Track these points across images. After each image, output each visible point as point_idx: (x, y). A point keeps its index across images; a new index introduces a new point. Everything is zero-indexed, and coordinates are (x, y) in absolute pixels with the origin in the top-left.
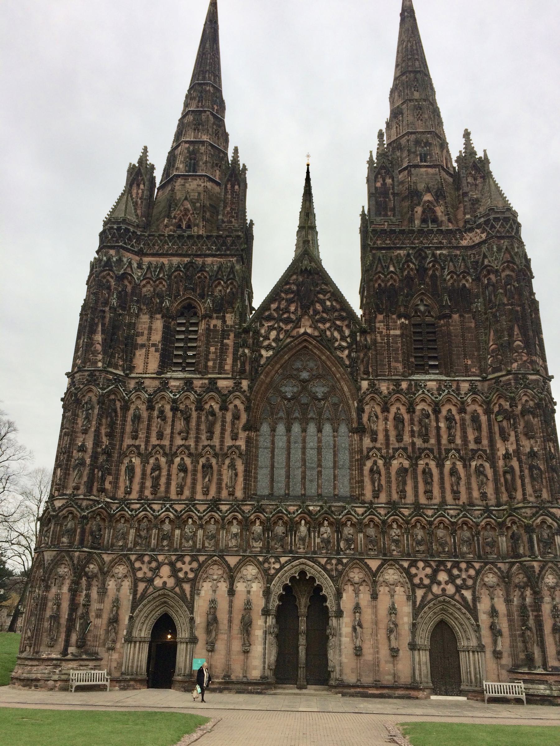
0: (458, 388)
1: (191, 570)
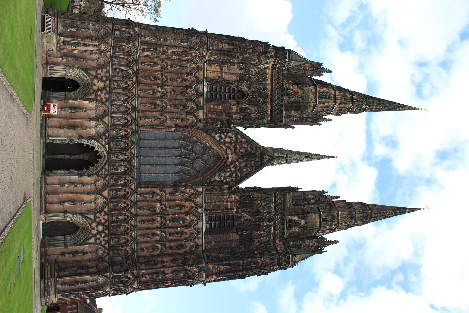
0: (198, 238)
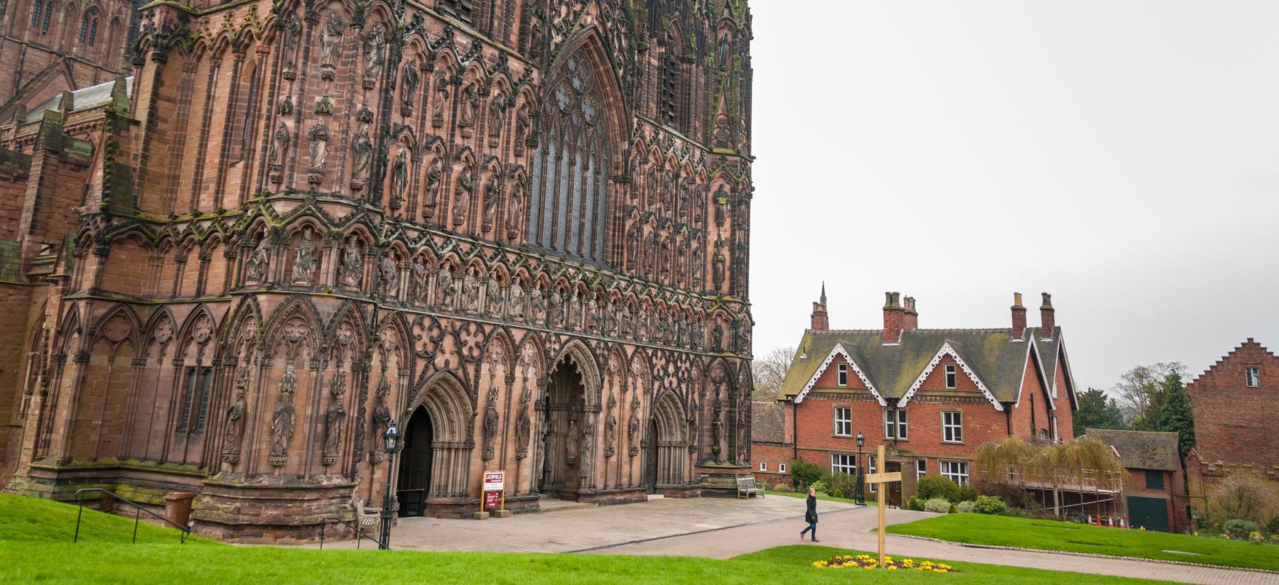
1: (477, 344)
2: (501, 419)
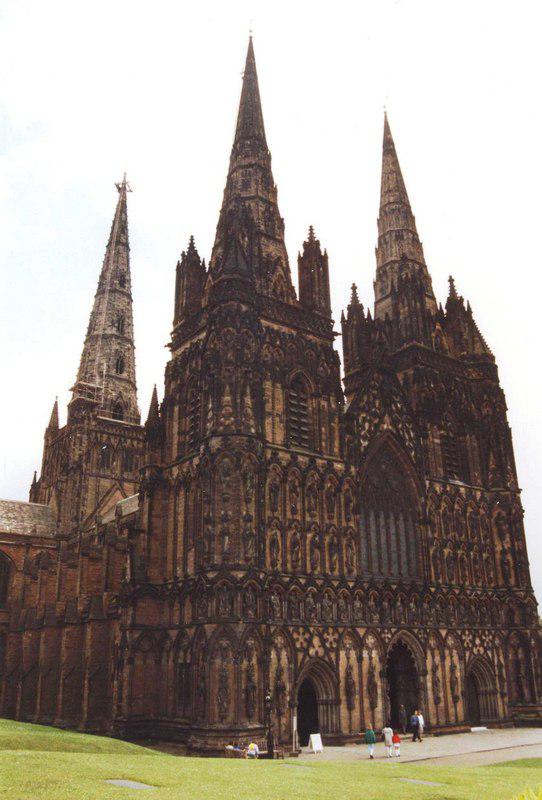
2: (357, 684)
